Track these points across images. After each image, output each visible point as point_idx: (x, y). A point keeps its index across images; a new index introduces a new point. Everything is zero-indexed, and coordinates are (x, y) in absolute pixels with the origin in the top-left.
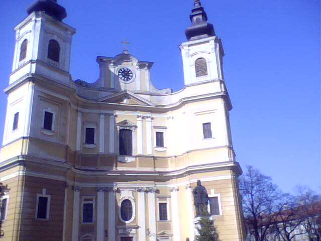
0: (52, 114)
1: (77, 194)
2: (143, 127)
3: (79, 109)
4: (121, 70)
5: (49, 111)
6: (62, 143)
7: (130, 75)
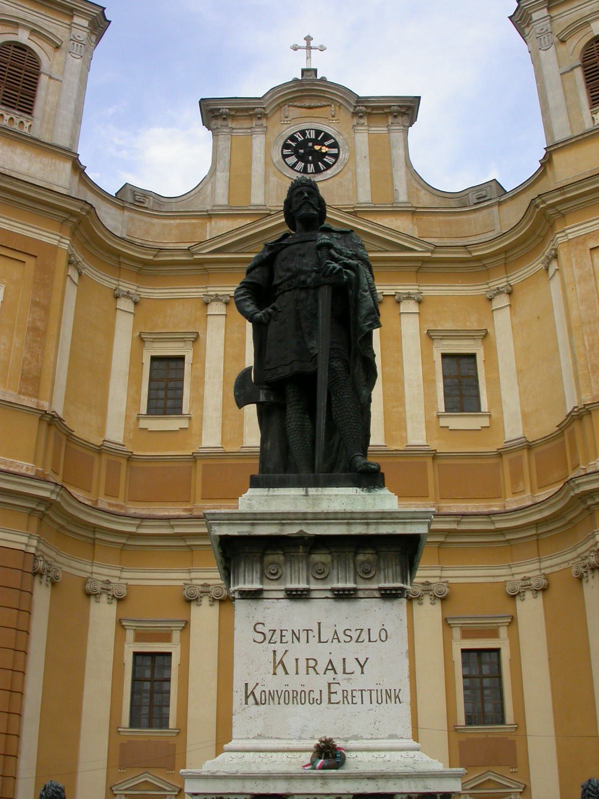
1: (103, 613)
3: (126, 286)
4: (292, 138)
6: (29, 402)
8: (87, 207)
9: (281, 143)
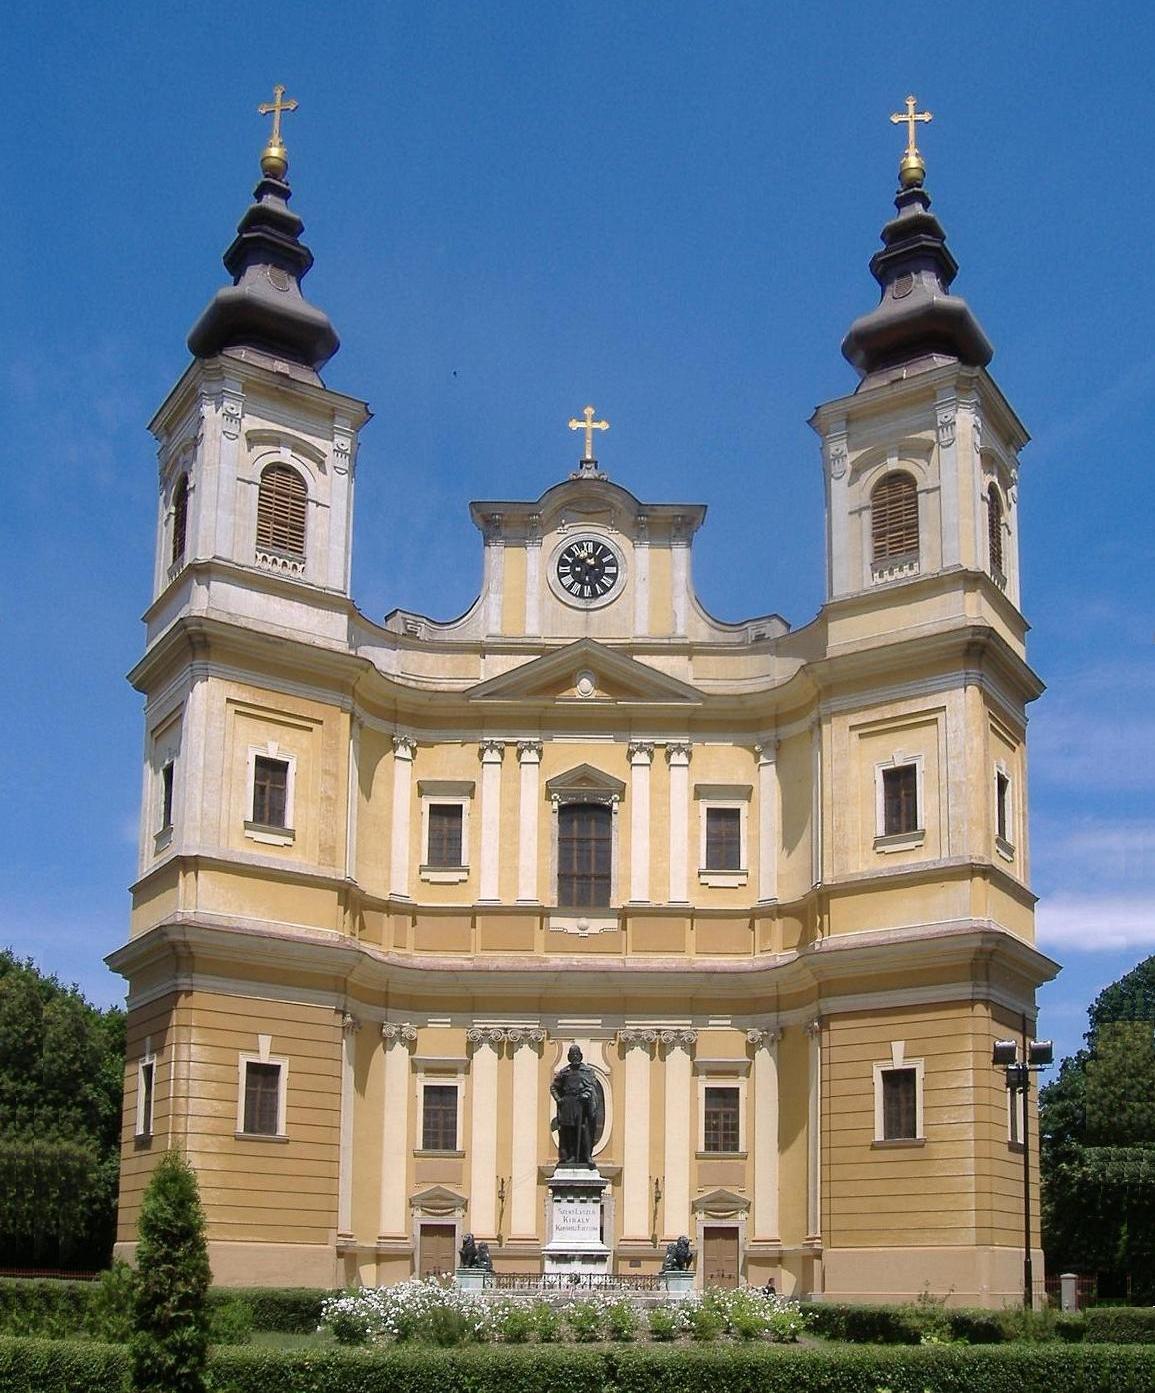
0: (282, 767)
2: (660, 794)
5: (272, 752)
7: (608, 570)
8: (366, 664)
9: (557, 559)
